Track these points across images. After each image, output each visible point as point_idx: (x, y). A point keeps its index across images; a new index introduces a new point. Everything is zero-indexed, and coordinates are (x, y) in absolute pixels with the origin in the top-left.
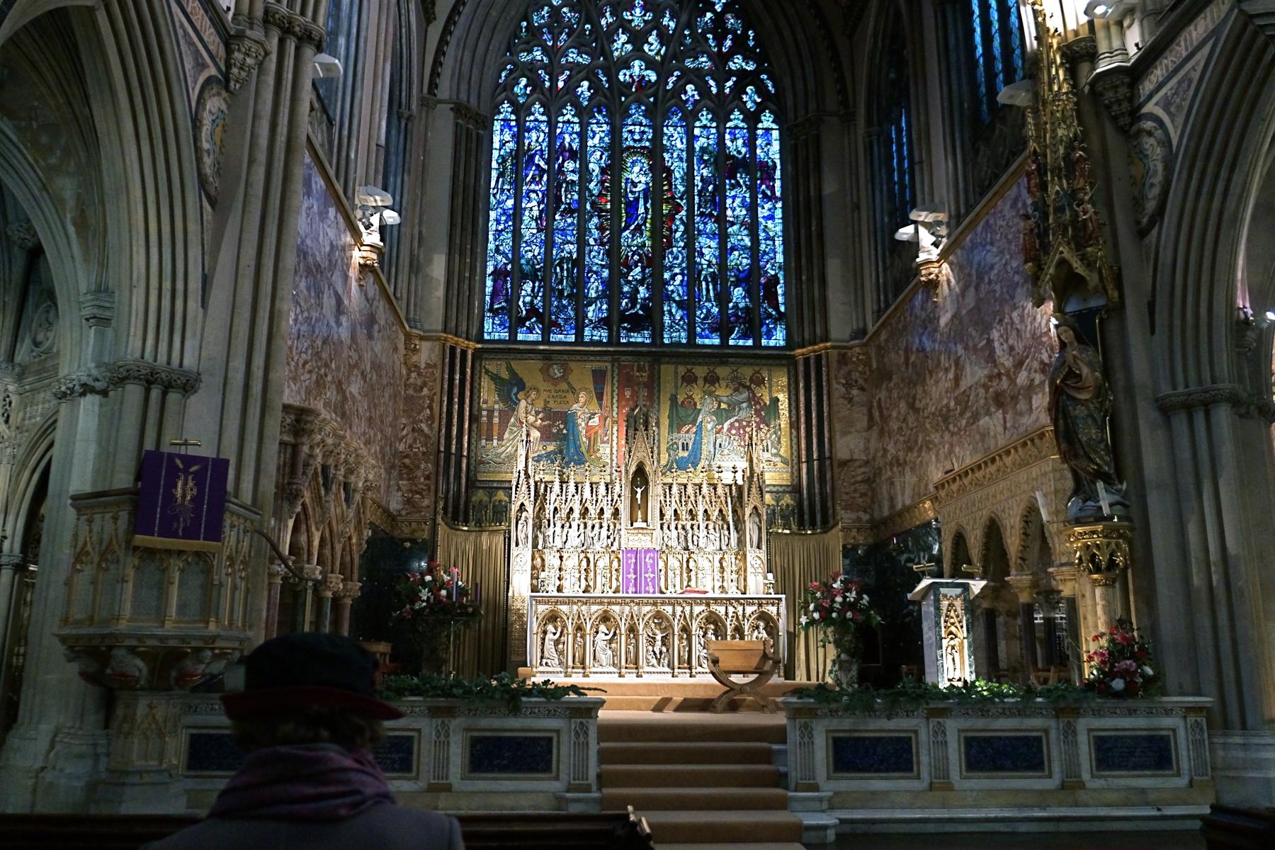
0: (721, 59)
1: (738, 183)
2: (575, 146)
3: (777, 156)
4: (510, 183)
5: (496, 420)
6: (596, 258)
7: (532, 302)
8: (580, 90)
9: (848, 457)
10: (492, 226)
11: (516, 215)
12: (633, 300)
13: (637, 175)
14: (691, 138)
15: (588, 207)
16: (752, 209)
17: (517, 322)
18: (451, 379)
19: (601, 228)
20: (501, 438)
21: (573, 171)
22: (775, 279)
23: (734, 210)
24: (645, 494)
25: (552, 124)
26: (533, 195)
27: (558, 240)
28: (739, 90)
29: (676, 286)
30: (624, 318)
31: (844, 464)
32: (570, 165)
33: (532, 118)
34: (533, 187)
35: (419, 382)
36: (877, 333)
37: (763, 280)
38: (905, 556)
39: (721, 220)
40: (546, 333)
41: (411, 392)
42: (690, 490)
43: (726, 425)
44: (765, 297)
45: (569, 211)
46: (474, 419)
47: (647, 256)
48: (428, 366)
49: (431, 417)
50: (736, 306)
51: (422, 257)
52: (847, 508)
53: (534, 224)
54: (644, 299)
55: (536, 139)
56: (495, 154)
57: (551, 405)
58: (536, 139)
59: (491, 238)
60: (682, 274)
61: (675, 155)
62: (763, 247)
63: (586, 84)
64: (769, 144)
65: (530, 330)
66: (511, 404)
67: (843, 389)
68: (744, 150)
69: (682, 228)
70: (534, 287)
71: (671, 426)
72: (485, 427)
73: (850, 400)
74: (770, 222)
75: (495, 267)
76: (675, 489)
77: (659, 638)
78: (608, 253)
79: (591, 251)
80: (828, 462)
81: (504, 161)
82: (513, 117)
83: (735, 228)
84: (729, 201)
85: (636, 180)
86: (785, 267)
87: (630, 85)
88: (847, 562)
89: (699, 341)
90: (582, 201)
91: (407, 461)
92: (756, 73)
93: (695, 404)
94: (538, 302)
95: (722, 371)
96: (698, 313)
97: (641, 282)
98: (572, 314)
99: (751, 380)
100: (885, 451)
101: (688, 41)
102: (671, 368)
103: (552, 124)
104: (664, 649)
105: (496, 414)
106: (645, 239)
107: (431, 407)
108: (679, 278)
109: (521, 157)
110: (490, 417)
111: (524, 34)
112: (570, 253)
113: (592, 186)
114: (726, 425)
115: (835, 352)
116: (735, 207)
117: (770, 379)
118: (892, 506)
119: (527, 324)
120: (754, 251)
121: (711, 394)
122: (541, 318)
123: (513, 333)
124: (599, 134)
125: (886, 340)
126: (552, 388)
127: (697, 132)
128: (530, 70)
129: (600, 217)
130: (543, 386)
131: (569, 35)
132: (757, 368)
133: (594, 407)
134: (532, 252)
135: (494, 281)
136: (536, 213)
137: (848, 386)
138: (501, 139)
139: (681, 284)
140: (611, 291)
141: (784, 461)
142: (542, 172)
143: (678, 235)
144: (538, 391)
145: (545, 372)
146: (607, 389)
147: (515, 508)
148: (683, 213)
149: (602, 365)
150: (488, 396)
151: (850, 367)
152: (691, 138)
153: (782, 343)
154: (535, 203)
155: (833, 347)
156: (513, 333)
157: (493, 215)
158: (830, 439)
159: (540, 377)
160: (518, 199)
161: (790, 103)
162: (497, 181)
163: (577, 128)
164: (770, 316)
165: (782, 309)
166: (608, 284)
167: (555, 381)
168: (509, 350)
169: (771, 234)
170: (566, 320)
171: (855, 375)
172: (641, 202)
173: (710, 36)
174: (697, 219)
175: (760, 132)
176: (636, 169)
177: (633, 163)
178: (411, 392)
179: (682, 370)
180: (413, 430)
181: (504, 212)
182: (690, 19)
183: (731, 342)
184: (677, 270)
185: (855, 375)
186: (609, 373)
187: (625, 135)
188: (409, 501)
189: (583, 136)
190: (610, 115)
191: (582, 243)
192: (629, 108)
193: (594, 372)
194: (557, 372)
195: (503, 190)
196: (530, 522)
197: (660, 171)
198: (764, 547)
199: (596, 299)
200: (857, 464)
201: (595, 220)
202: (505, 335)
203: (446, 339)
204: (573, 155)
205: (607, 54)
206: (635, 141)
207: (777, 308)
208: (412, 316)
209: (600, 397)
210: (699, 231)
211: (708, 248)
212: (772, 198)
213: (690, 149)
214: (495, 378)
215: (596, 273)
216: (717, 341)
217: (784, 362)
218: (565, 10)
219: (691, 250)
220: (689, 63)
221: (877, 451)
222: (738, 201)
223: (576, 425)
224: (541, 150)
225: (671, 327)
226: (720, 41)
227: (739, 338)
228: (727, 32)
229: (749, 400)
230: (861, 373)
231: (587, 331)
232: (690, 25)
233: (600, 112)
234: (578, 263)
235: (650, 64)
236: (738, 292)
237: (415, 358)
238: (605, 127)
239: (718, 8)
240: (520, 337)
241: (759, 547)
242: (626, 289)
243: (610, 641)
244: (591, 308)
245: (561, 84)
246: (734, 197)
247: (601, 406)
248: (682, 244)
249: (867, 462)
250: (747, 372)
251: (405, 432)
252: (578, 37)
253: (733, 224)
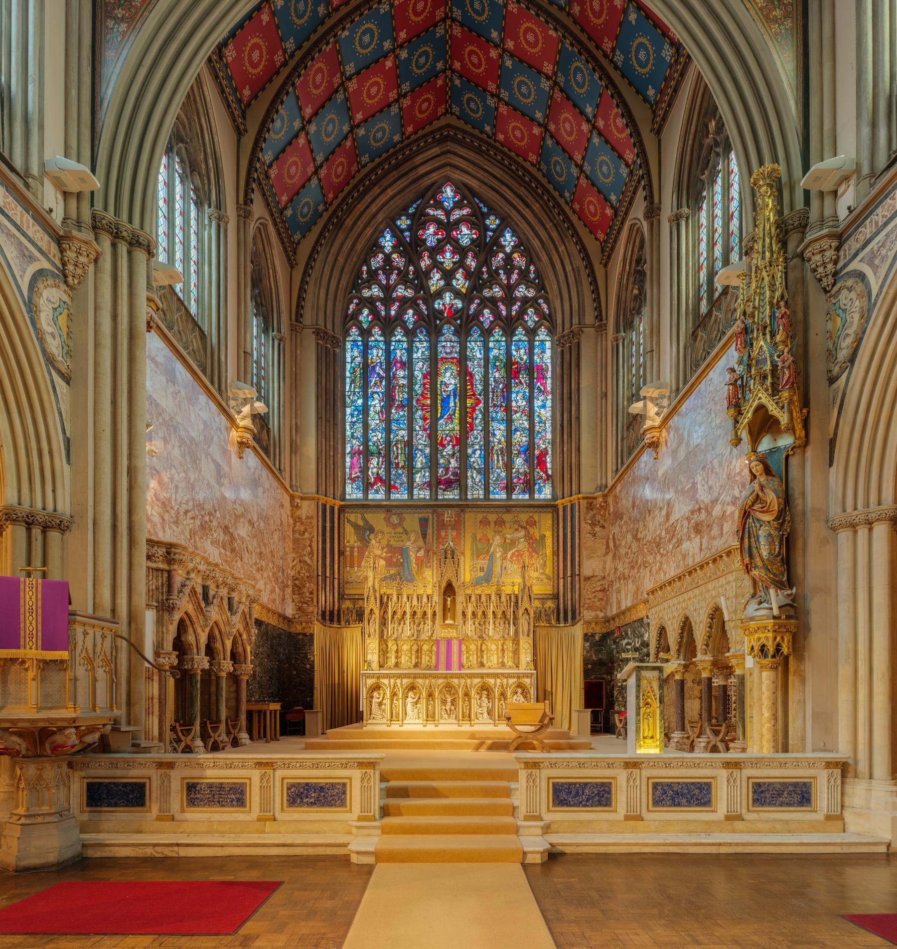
0: (509, 289)
1: (521, 382)
2: (404, 359)
3: (549, 361)
4: (360, 388)
5: (356, 554)
6: (421, 440)
8: (406, 316)
9: (591, 574)
10: (348, 419)
11: (365, 410)
12: (447, 469)
13: (449, 379)
14: (487, 350)
15: (414, 403)
16: (530, 400)
17: (367, 486)
18: (324, 527)
19: (425, 419)
20: (359, 566)
21: (403, 377)
23: (517, 402)
24: (454, 601)
25: (388, 343)
26: (376, 396)
27: (394, 428)
28: (522, 312)
29: (476, 458)
30: (439, 482)
31: (587, 579)
32: (401, 373)
33: (373, 339)
34: (375, 390)
35: (302, 529)
36: (614, 486)
37: (537, 452)
38: (626, 641)
39: (508, 410)
40: (388, 492)
41: (297, 535)
42: (483, 599)
43: (509, 555)
44: (538, 464)
45: (402, 406)
46: (341, 553)
47: (456, 438)
48: (308, 517)
49: (311, 553)
51: (298, 441)
52: (590, 608)
53: (377, 416)
55: (377, 355)
56: (348, 366)
57: (392, 543)
58: (377, 355)
59: (348, 427)
60: (481, 450)
61: (476, 363)
62: (537, 428)
63: (411, 312)
64: (543, 352)
65: (377, 492)
66: (365, 542)
67: (589, 528)
68: (525, 357)
69: (480, 416)
71: (472, 554)
72: (348, 559)
73: (594, 535)
74: (542, 410)
75: (352, 447)
76: (473, 598)
78: (429, 436)
79: (417, 435)
80: (577, 578)
81: (354, 371)
82: (360, 339)
83: (518, 415)
84: (514, 395)
86: (553, 443)
87: (441, 312)
88: (588, 644)
89: (491, 497)
90: (410, 398)
91: (297, 582)
92: (534, 300)
93: (489, 540)
94: (382, 472)
95: (507, 517)
96: (491, 476)
97: (453, 456)
98: (405, 480)
99: (527, 522)
100: (616, 569)
101: (485, 276)
102: (473, 515)
103: (388, 343)
105: (356, 550)
106: (455, 425)
107: (311, 546)
108: (478, 452)
109: (366, 368)
110: (352, 552)
111: (365, 276)
112: (403, 437)
113: (417, 387)
114: (509, 555)
115: (585, 501)
116: (519, 400)
117: (540, 522)
118: (619, 607)
119: (375, 487)
120: (531, 431)
121: (499, 532)
122: (383, 482)
124: (421, 349)
126: (392, 531)
127: (491, 345)
128: (370, 302)
129: (422, 410)
130: (386, 530)
131: (398, 275)
132: (531, 515)
133: (421, 543)
134: (377, 437)
135: (352, 458)
136: (378, 409)
137: (593, 525)
138: (352, 355)
139: (480, 457)
140: (433, 463)
141: (548, 578)
142: (381, 378)
143: (477, 421)
144: (383, 533)
145: (387, 520)
146: (430, 531)
147: (367, 612)
148: (481, 405)
149: (426, 516)
150: (350, 537)
151: (595, 511)
152: (487, 350)
153: (549, 497)
154: (377, 401)
155: (584, 498)
156: (366, 493)
157: (348, 411)
158: (579, 562)
159: (384, 523)
160: (366, 397)
161: (559, 321)
162: (350, 386)
163: (405, 345)
164: (541, 478)
165: (550, 472)
167: (395, 526)
168: (363, 506)
169: (544, 418)
170: (401, 484)
171: (598, 517)
172: (452, 398)
173: (501, 272)
174: (491, 409)
175: (537, 343)
176: (448, 374)
177: (446, 370)
178: (297, 535)
179: (480, 517)
180: (300, 561)
182: (486, 259)
183: (514, 497)
184: (477, 447)
185: (598, 517)
186: (430, 520)
187: (440, 349)
188: (300, 609)
189: (410, 351)
190: (429, 334)
191: (411, 430)
192: (442, 327)
193: (420, 519)
194: (395, 519)
196: (377, 621)
197: (464, 374)
198: (531, 636)
199: (422, 468)
200: (597, 579)
201: (420, 412)
202: (360, 495)
203: (318, 499)
204: (403, 365)
205: (426, 289)
206: (447, 353)
207: (546, 473)
208: (294, 483)
209: (424, 536)
210: (492, 418)
211: (499, 431)
212: (544, 392)
213: (486, 359)
214: (355, 526)
215: (421, 450)
217: (550, 510)
218: (395, 256)
219: (487, 432)
220: (487, 293)
221: (611, 569)
223: (408, 556)
224: (381, 363)
225: (473, 487)
226: (509, 275)
228: (513, 268)
229: (525, 536)
230: (602, 515)
231: (415, 492)
232: (487, 262)
233: (421, 332)
234: (409, 444)
235: (457, 294)
236: (519, 462)
237: (298, 513)
238: (425, 344)
239: (508, 250)
241: (528, 635)
242: (441, 461)
245: (393, 313)
246: (518, 393)
247: (425, 542)
248: (480, 428)
249: (604, 577)
250: (524, 517)
251: (295, 563)
252: (404, 277)
253: (516, 412)
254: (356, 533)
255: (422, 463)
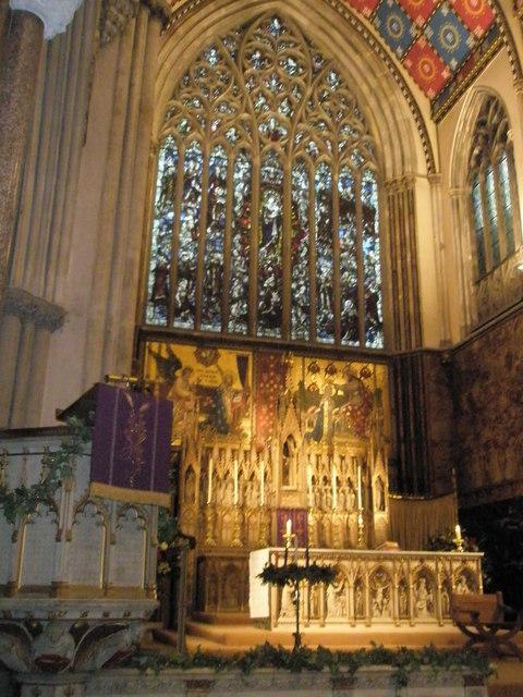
1: (347, 220)
7: (186, 297)
10: (156, 231)
16: (356, 239)
22: (374, 298)
23: (345, 240)
26: (189, 211)
50: (346, 314)
53: (189, 235)
54: (276, 303)
56: (160, 175)
59: (154, 241)
64: (370, 193)
65: (185, 319)
70: (188, 285)
75: (157, 265)
77: (380, 590)
78: (248, 264)
79: (235, 260)
83: (346, 254)
85: (271, 209)
89: (319, 339)
95: (339, 365)
97: (274, 289)
99: (362, 375)
104: (385, 600)
105: (157, 387)
108: (303, 288)
113: (237, 208)
116: (344, 237)
119: (182, 314)
122: (193, 310)
123: (170, 322)
125: (480, 349)
129: (242, 234)
135: (157, 277)
136: (191, 226)
142: (197, 194)
143: (303, 254)
149: (245, 353)
153: (381, 346)
154: (190, 217)
156: (170, 322)
157: (157, 223)
164: (372, 324)
165: (381, 320)
166: (246, 287)
169: (372, 262)
172: (275, 226)
176: (271, 200)
177: (269, 196)
179: (308, 361)
181: (166, 222)
183: (343, 342)
195: (165, 205)
202: (163, 321)
207: (377, 318)
212: (370, 233)
214: (158, 358)
216: (332, 341)
222: (348, 233)
227: (349, 340)
240: (176, 324)
243: (339, 594)
244: (234, 306)
246: (345, 231)
253: (343, 251)
254: (159, 367)
255: (239, 293)
